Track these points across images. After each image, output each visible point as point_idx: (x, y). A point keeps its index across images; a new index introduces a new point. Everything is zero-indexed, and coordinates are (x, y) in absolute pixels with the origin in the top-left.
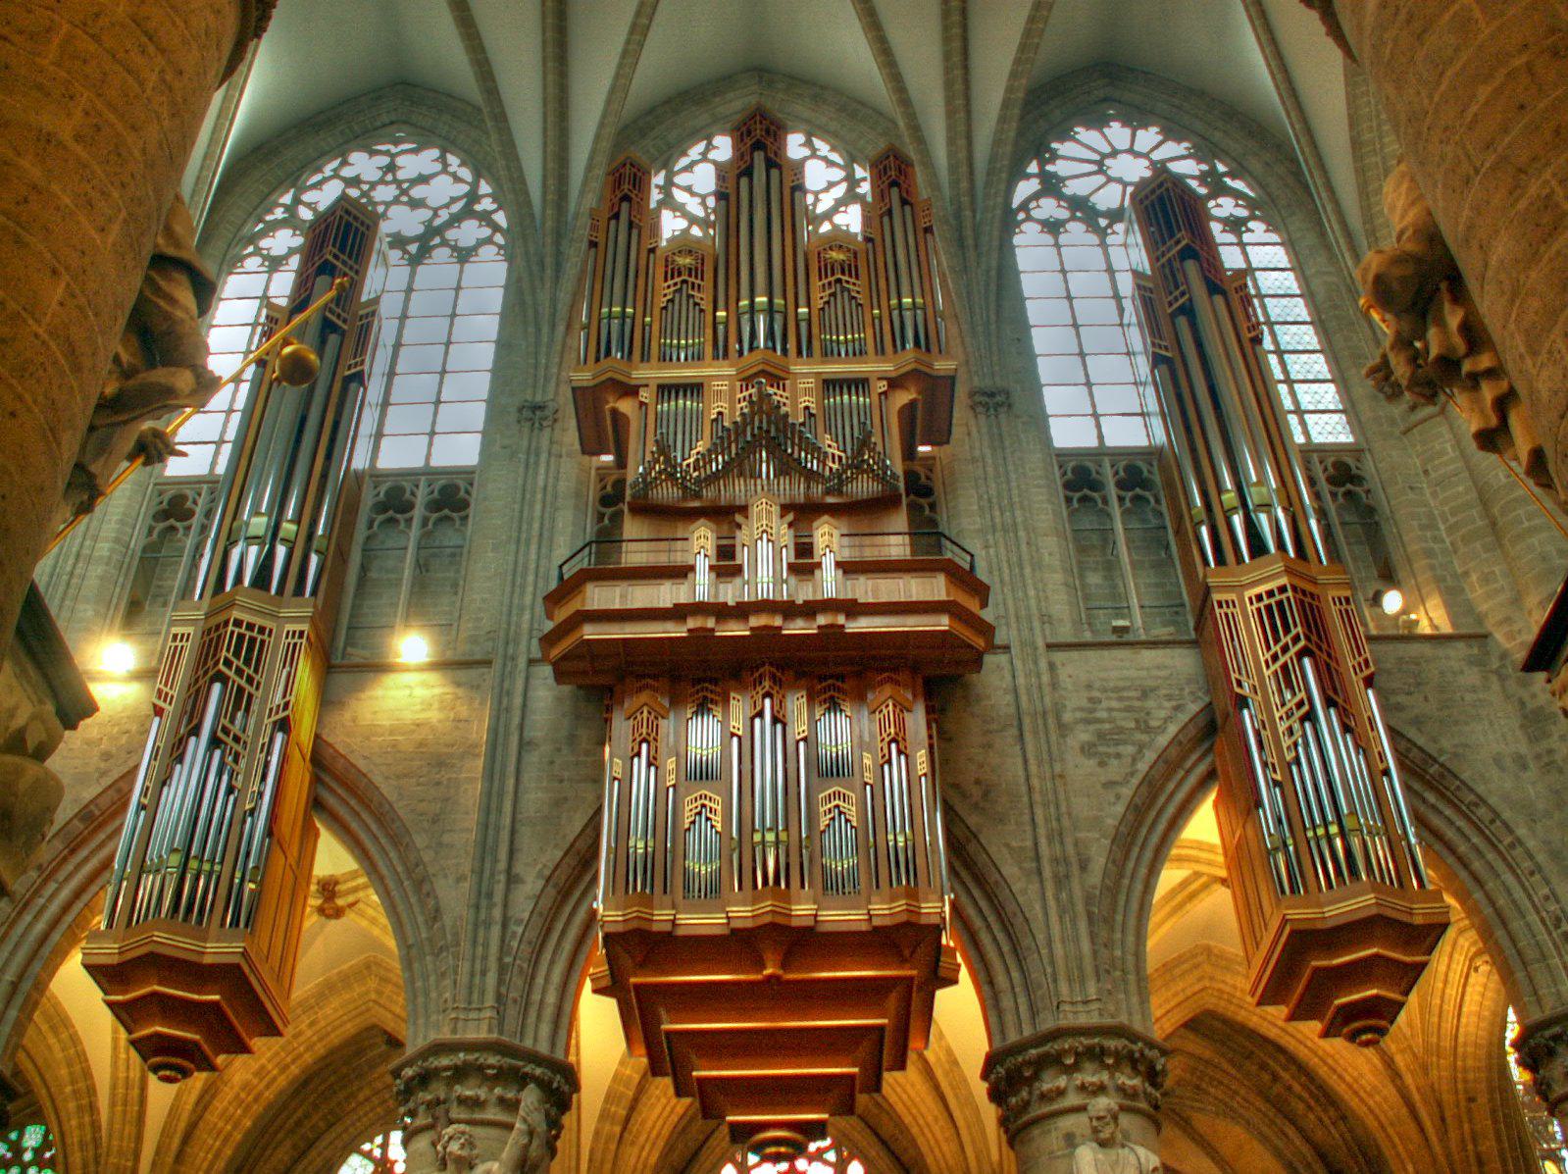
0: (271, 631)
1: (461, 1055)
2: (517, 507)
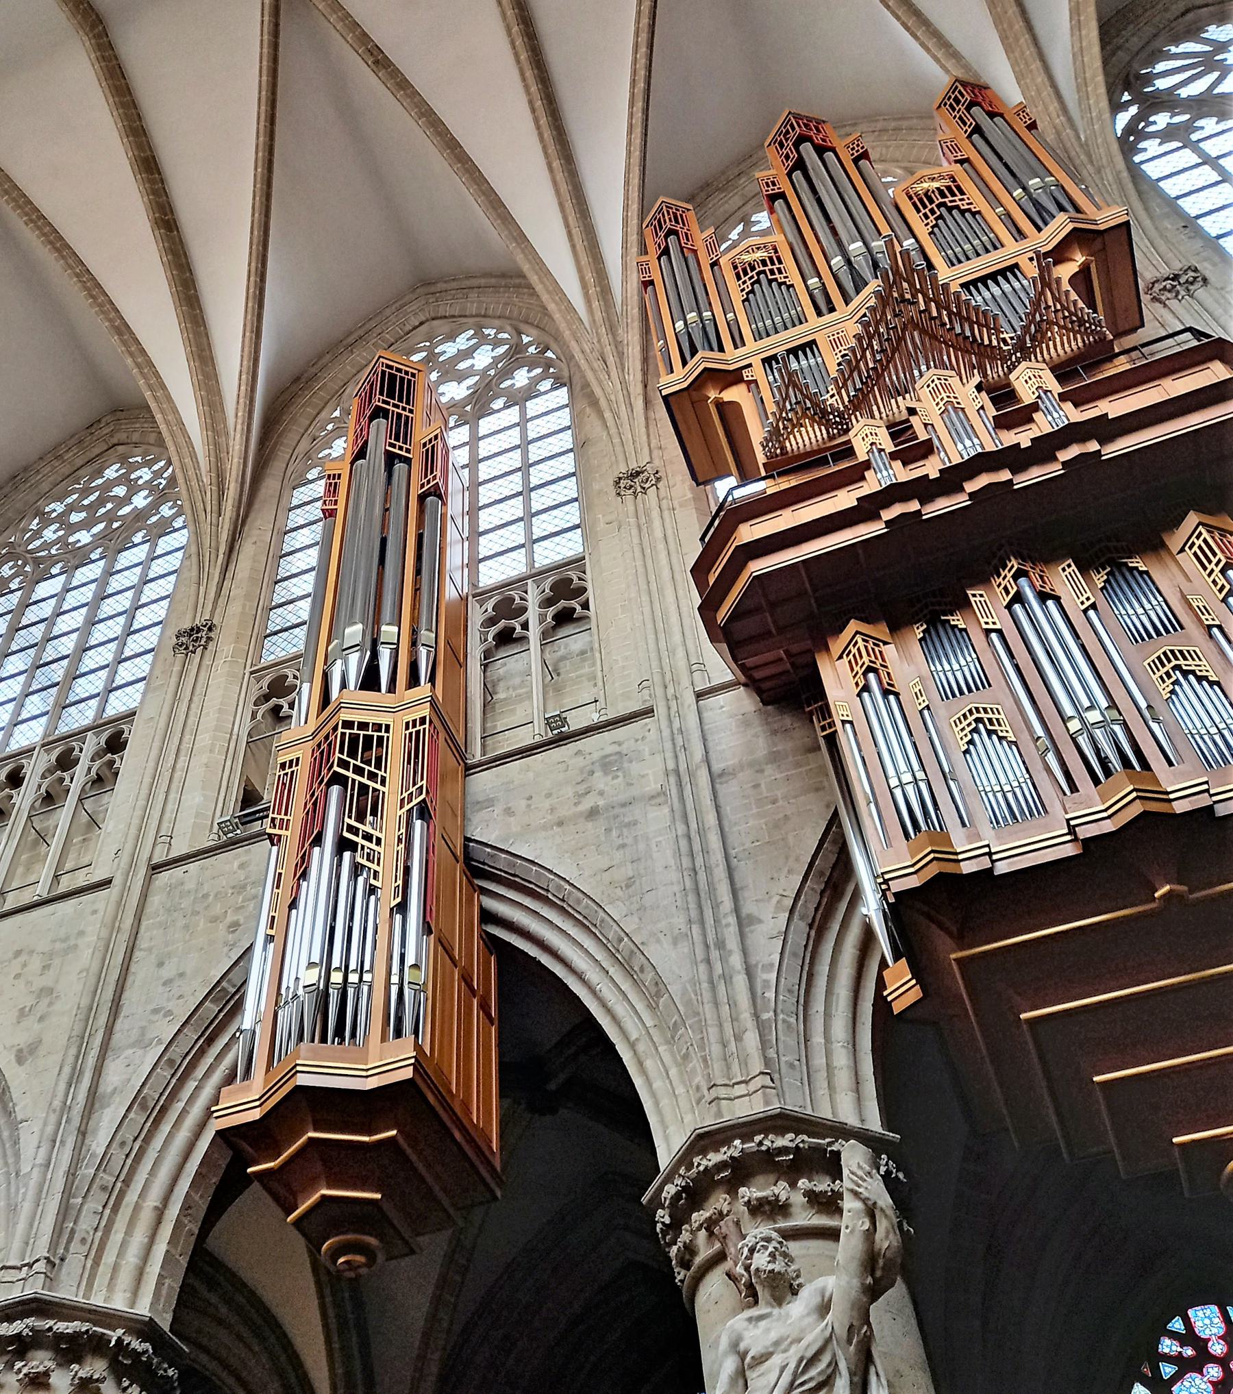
0: (388, 727)
1: (737, 1142)
2: (639, 563)
